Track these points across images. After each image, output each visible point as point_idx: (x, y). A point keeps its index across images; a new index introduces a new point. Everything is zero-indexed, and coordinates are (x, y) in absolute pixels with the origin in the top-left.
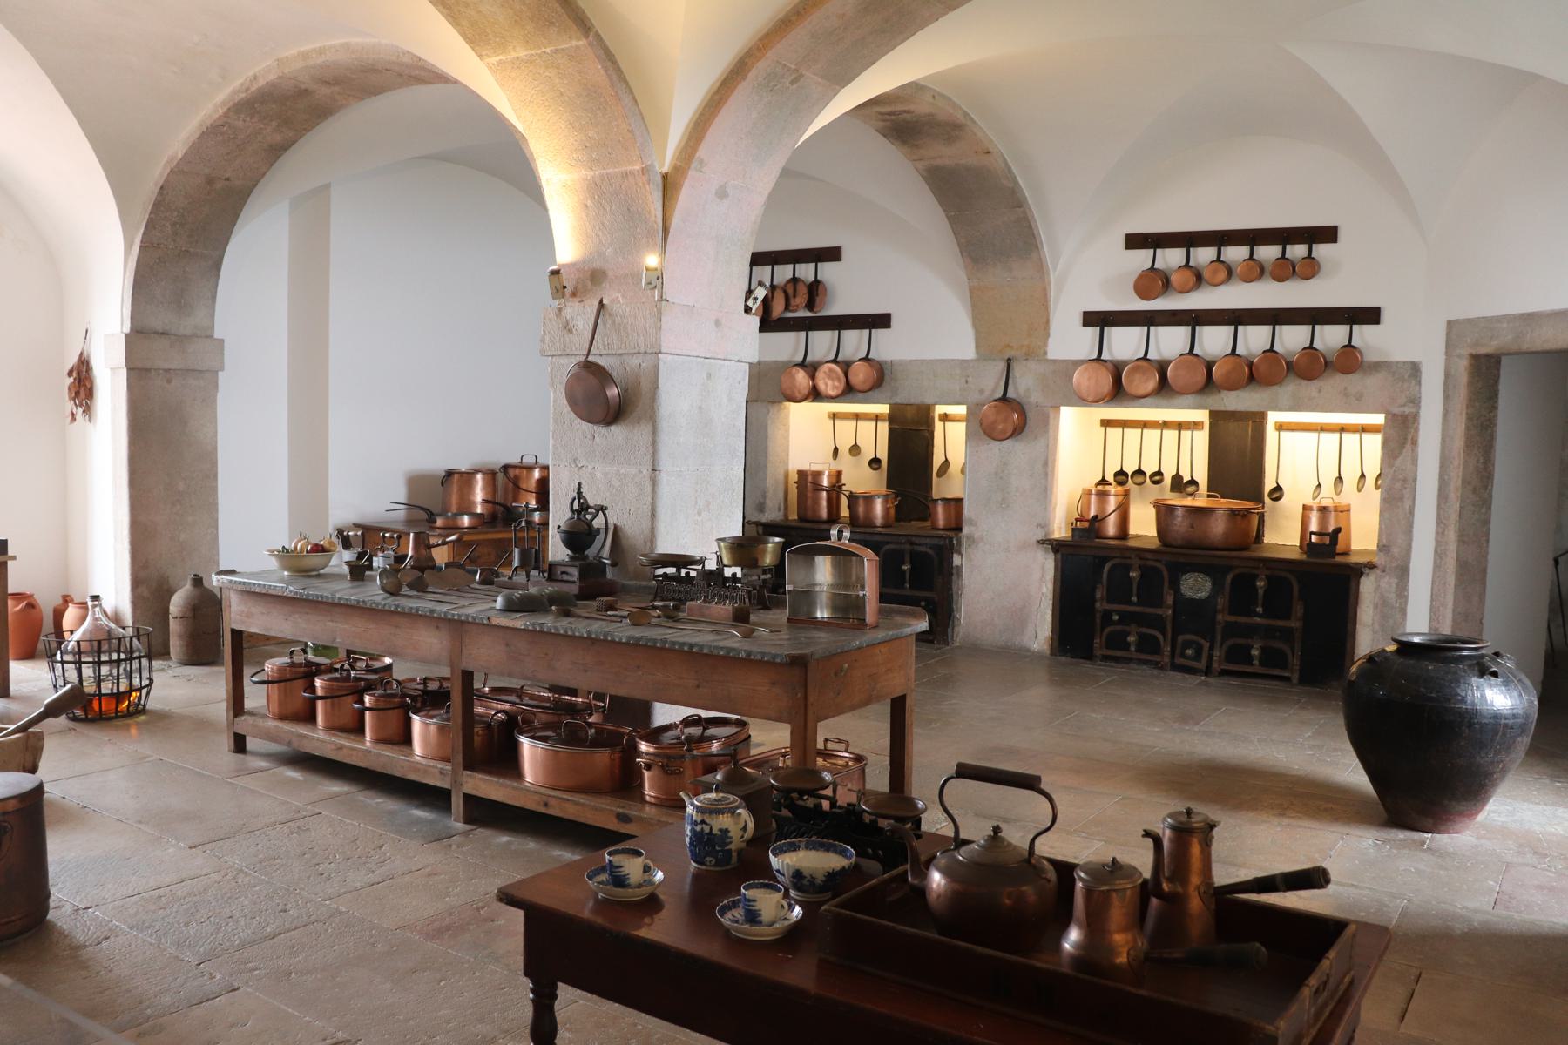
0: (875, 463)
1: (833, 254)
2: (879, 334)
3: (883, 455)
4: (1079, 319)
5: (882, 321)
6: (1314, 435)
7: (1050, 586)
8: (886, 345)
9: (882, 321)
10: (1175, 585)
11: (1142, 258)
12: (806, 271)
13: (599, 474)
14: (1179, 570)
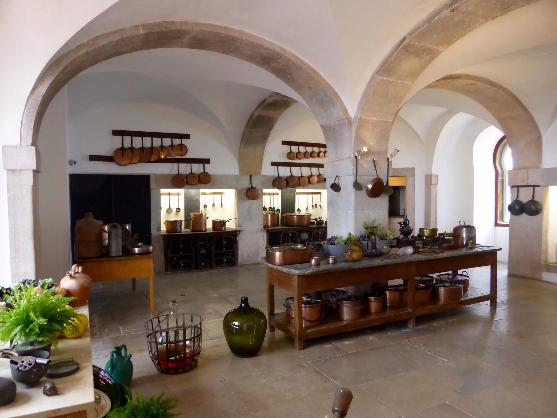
0: (178, 210)
1: (187, 137)
2: (206, 165)
3: (182, 207)
4: (270, 164)
5: (207, 161)
6: (306, 196)
7: (266, 242)
8: (210, 169)
9: (207, 161)
10: (300, 236)
11: (286, 148)
12: (177, 141)
13: (371, 214)
14: (300, 232)
